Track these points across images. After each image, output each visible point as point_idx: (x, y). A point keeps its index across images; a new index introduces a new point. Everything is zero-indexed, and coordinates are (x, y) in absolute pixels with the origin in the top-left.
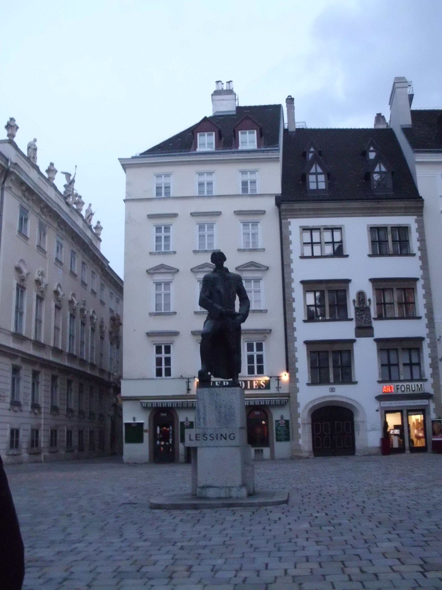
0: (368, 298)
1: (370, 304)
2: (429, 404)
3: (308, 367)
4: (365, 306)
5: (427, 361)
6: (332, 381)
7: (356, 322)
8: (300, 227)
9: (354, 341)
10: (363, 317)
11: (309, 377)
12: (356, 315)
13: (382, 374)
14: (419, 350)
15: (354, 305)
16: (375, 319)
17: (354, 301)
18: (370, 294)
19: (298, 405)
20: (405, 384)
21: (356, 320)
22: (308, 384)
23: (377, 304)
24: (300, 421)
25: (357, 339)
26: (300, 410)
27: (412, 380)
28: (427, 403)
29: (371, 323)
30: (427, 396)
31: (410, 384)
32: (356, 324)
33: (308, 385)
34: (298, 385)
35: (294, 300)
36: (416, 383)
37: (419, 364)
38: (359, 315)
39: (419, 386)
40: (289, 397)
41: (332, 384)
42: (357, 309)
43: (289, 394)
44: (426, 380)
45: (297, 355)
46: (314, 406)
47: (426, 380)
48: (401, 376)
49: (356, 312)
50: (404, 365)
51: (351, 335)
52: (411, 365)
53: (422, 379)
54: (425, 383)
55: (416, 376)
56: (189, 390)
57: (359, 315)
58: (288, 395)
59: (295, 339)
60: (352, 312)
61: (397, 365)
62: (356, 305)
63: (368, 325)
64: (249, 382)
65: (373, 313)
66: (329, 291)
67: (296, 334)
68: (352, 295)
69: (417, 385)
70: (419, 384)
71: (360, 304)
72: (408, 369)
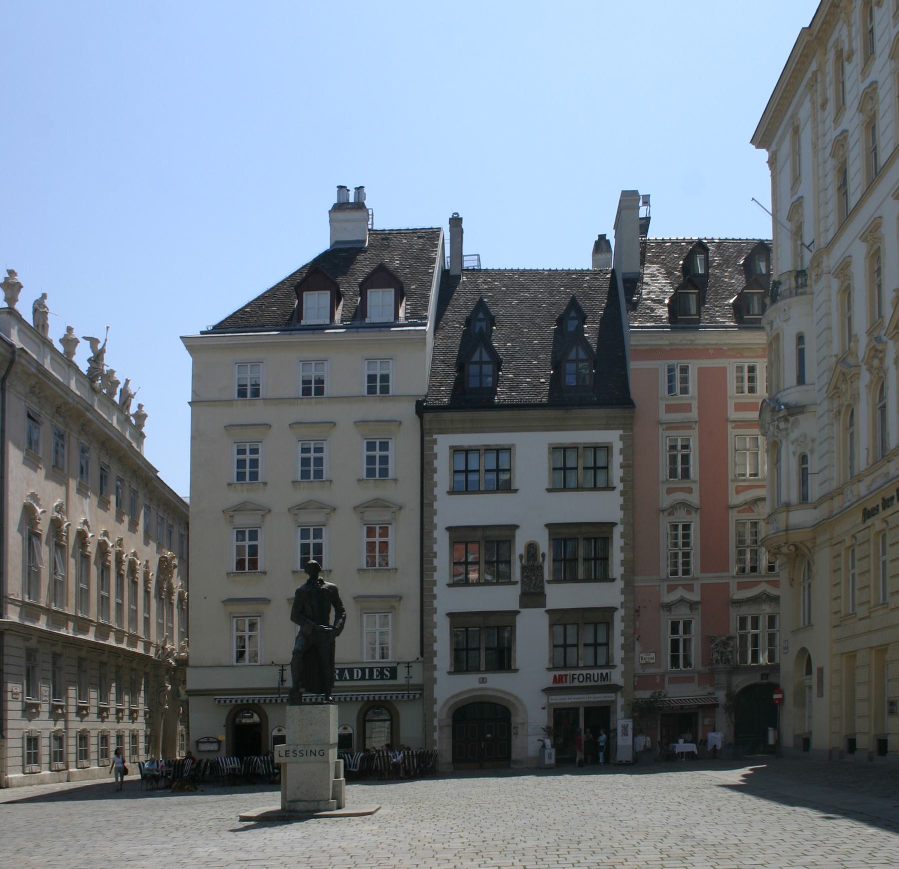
0: (541, 552)
1: (544, 560)
2: (616, 699)
3: (451, 649)
4: (536, 564)
5: (618, 640)
6: (483, 668)
7: (522, 587)
8: (451, 447)
9: (517, 612)
10: (532, 580)
11: (451, 663)
12: (522, 576)
13: (552, 659)
14: (609, 625)
15: (521, 562)
16: (549, 582)
17: (521, 557)
18: (544, 546)
19: (435, 701)
20: (584, 672)
21: (522, 584)
22: (450, 673)
23: (554, 561)
24: (436, 722)
25: (521, 610)
26: (437, 708)
27: (596, 666)
28: (613, 699)
29: (543, 587)
30: (614, 688)
31: (591, 672)
32: (522, 590)
33: (449, 675)
34: (436, 674)
35: (435, 555)
36: (600, 671)
37: (607, 644)
38: (526, 577)
39: (604, 675)
40: (422, 690)
41: (483, 672)
42: (524, 569)
43: (423, 685)
44: (614, 667)
45: (436, 632)
46: (456, 703)
47: (614, 667)
48: (580, 661)
49: (522, 573)
50: (585, 645)
51: (514, 605)
52: (595, 645)
53: (609, 665)
54: (612, 670)
55: (601, 661)
56: (283, 680)
57: (526, 577)
58: (420, 688)
59: (435, 611)
60: (517, 574)
61: (577, 645)
62: (523, 562)
63: (539, 590)
64: (367, 670)
65: (547, 576)
66: (486, 541)
67: (436, 603)
68: (520, 548)
69: (602, 674)
70: (604, 672)
71: (528, 560)
72: (591, 650)
